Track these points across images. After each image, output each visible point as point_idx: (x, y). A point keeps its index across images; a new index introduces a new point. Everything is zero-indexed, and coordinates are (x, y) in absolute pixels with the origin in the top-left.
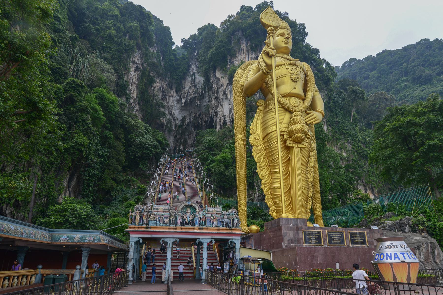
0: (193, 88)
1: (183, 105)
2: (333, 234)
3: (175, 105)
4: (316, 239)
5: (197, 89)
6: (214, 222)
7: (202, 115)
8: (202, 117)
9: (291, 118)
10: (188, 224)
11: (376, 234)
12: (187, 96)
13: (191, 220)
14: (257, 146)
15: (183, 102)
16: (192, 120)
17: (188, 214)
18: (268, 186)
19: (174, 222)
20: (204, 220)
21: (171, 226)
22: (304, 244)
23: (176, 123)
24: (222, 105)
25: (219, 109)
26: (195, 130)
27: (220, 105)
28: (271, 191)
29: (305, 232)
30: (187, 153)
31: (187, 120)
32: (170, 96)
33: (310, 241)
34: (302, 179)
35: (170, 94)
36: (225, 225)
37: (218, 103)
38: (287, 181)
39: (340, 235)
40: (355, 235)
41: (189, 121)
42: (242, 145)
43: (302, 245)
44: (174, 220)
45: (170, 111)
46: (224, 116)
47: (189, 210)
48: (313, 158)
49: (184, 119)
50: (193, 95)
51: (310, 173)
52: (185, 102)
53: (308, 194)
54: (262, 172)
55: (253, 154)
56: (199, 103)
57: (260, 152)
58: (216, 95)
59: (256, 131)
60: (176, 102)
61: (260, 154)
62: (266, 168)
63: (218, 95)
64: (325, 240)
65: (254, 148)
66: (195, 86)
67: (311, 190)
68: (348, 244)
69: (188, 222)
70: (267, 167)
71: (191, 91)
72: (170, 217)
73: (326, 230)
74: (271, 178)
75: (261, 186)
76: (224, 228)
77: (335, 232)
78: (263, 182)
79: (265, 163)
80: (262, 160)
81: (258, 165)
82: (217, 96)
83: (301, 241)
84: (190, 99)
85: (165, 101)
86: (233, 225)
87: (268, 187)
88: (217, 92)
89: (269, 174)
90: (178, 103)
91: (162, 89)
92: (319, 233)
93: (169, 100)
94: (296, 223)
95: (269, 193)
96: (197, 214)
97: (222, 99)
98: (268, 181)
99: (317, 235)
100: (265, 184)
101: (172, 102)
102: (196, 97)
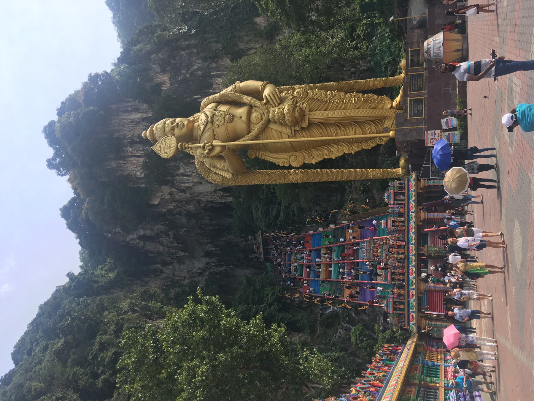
0: (161, 239)
1: (187, 254)
2: (413, 87)
3: (187, 266)
4: (418, 104)
5: (161, 232)
7: (202, 224)
8: (205, 224)
12: (173, 248)
14: (304, 158)
15: (182, 254)
16: (209, 241)
23: (214, 265)
24: (199, 194)
25: (203, 199)
26: (225, 236)
27: (198, 198)
28: (357, 142)
31: (209, 247)
32: (174, 274)
33: (420, 111)
34: (344, 109)
35: (171, 275)
37: (193, 200)
38: (346, 125)
39: (413, 78)
40: (413, 61)
41: (210, 245)
43: (425, 119)
45: (195, 275)
46: (216, 191)
49: (208, 254)
50: (171, 239)
52: (182, 251)
54: (334, 152)
55: (314, 163)
56: (184, 229)
57: (312, 154)
58: (184, 203)
59: (286, 159)
60: (182, 266)
61: (313, 155)
62: (330, 148)
63: (183, 201)
65: (306, 162)
66: (157, 235)
67: (355, 95)
70: (328, 146)
71: (165, 240)
73: (409, 93)
74: (342, 142)
75: (351, 153)
77: (410, 84)
78: (346, 152)
80: (320, 153)
81: (326, 157)
82: (184, 203)
84: (178, 243)
85: (182, 282)
87: (353, 146)
88: (179, 201)
89: (337, 145)
90: (184, 264)
91: (165, 286)
93: (180, 276)
95: (360, 144)
97: (189, 194)
98: (346, 146)
100: (349, 149)
101: (183, 271)
102: (174, 235)
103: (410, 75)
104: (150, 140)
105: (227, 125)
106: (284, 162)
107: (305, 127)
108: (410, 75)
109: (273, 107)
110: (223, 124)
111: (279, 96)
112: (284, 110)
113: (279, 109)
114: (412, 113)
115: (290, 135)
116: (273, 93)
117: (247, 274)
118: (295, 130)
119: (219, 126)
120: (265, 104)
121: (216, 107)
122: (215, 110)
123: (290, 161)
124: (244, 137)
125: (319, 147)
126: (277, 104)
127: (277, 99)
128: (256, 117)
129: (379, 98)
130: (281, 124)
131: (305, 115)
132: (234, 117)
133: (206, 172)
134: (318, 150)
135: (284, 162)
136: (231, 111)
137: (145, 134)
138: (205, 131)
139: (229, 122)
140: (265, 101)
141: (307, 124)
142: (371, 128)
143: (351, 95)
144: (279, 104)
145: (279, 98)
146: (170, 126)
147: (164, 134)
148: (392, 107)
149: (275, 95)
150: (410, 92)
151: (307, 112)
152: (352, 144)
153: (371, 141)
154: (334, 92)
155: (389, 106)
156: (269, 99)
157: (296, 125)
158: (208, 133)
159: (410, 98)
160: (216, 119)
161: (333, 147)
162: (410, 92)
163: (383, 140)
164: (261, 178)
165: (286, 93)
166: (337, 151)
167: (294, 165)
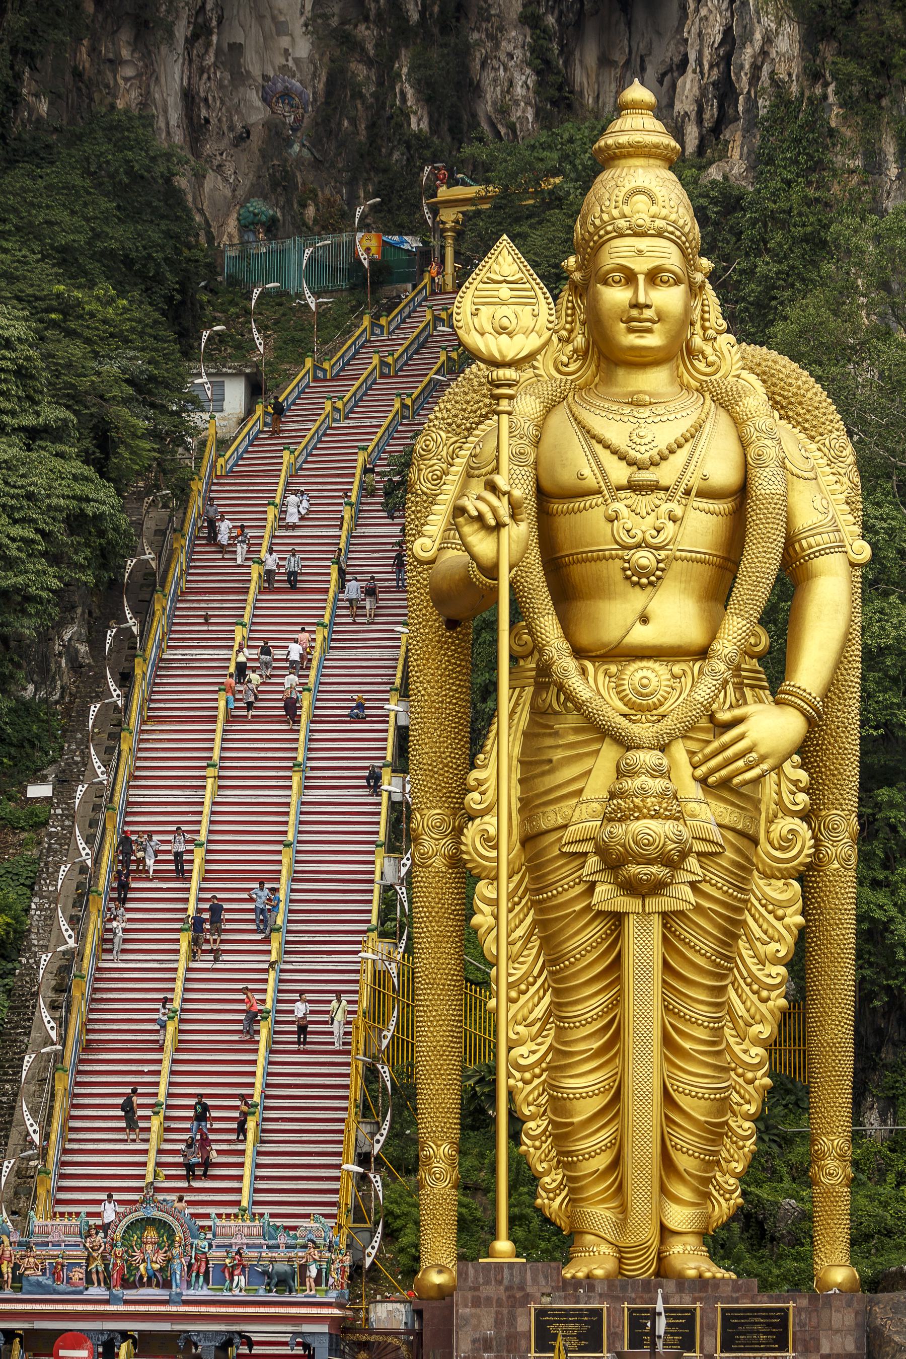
4: (580, 1337)
6: (236, 1278)
9: (621, 773)
10: (149, 1284)
11: (838, 1311)
13: (161, 1270)
17: (149, 1248)
18: (539, 1076)
19: (101, 1276)
20: (203, 1269)
21: (96, 1291)
22: (532, 1354)
29: (540, 1313)
30: (449, 216)
36: (276, 1286)
39: (681, 1317)
40: (747, 1317)
42: (439, 863)
44: (100, 1269)
47: (151, 1235)
48: (789, 911)
51: (764, 994)
53: (723, 1105)
54: (514, 1008)
55: (476, 920)
64: (615, 1336)
67: (757, 1082)
68: (708, 1349)
69: (149, 1278)
72: (89, 1259)
73: (626, 1305)
76: (273, 1297)
79: (525, 968)
83: (523, 1343)
86: (303, 1283)
92: (598, 1313)
94: (516, 1280)
96: (175, 1252)
99: (586, 1322)
103: (695, 1309)
104: (602, 143)
105: (612, 558)
106: (483, 788)
107: (594, 901)
108: (695, 1309)
109: (691, 753)
110: (617, 543)
111: (736, 781)
112: (652, 817)
113: (663, 795)
114: (549, 1316)
115: (567, 835)
116: (750, 750)
117: (285, 42)
118: (585, 854)
119: (612, 521)
120: (712, 718)
121: (704, 494)
122: (687, 493)
123: (487, 819)
124: (568, 635)
125: (538, 943)
126: (699, 772)
127: (723, 773)
128: (644, 686)
129: (732, 1181)
130: (612, 795)
131: (643, 898)
132: (650, 588)
133: (464, 410)
134: (528, 938)
135: (483, 788)
136: (677, 566)
137: (636, 106)
138: (598, 448)
139: (624, 570)
140: (725, 716)
141: (604, 907)
142: (591, 1157)
143: (760, 1065)
144: (703, 781)
145: (729, 779)
146: (641, 266)
147: (607, 233)
148: (665, 1232)
149: (740, 763)
150: (629, 1309)
151: (655, 904)
152: (545, 1081)
153: (553, 1153)
154: (778, 996)
155: (672, 1225)
156: (727, 737)
157: (603, 860)
158: (587, 472)
159: (605, 1310)
160: (643, 502)
161: (536, 999)
162: (629, 1309)
163: (553, 1200)
164: (429, 682)
165: (795, 783)
166: (519, 1017)
167: (471, 832)
